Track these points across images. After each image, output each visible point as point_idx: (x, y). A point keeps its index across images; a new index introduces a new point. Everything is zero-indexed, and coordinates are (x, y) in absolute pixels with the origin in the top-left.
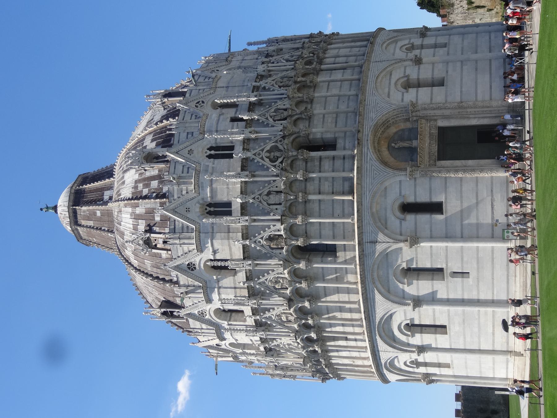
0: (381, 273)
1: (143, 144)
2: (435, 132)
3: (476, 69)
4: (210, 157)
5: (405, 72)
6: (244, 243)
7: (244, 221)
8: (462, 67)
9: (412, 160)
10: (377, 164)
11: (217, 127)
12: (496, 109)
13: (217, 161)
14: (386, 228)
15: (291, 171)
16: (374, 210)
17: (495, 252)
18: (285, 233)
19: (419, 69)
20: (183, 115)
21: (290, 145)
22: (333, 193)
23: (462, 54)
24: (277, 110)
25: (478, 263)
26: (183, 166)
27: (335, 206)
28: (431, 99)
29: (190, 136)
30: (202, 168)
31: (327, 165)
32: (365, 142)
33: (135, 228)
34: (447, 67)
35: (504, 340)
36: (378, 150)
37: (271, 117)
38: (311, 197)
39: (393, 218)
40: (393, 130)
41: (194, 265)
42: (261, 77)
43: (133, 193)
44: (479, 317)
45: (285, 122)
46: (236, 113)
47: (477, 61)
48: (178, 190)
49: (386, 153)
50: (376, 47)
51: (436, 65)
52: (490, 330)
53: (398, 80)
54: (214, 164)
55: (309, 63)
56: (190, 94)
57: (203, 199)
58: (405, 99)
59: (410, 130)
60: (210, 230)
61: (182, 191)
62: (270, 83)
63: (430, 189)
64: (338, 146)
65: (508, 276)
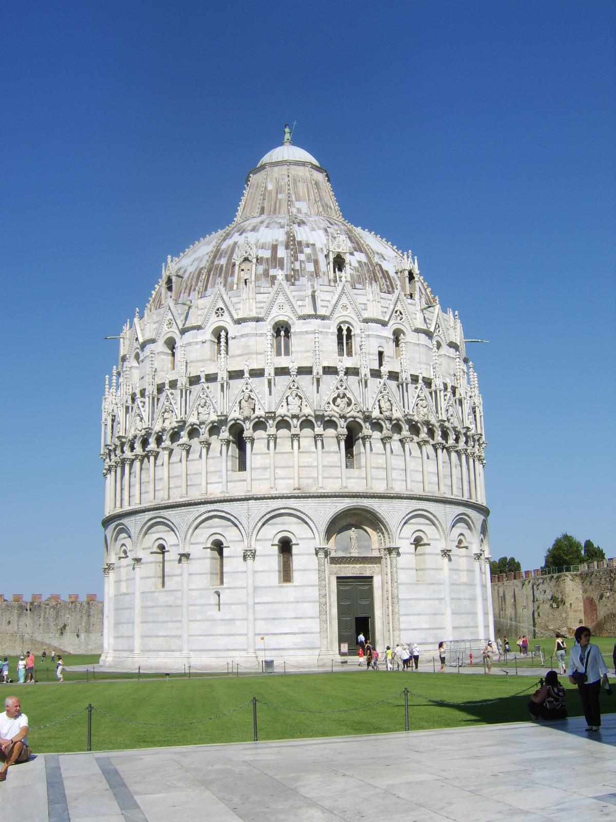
0: (216, 520)
1: (356, 251)
2: (368, 574)
3: (435, 614)
4: (340, 330)
6: (245, 371)
7: (269, 371)
8: (437, 599)
12: (392, 635)
13: (335, 338)
14: (263, 524)
16: (282, 511)
17: (241, 637)
18: (257, 417)
19: (436, 554)
22: (299, 467)
23: (452, 599)
25: (230, 620)
26: (329, 301)
27: (287, 469)
28: (402, 569)
29: (363, 307)
32: (355, 500)
34: (438, 584)
35: (151, 647)
36: (347, 514)
41: (222, 315)
42: (428, 383)
43: (300, 243)
44: (174, 622)
46: (388, 357)
48: (302, 296)
52: (161, 633)
54: (332, 335)
55: (445, 436)
56: (411, 304)
58: (402, 541)
60: (260, 332)
61: (301, 300)
63: (305, 570)
65: (217, 650)
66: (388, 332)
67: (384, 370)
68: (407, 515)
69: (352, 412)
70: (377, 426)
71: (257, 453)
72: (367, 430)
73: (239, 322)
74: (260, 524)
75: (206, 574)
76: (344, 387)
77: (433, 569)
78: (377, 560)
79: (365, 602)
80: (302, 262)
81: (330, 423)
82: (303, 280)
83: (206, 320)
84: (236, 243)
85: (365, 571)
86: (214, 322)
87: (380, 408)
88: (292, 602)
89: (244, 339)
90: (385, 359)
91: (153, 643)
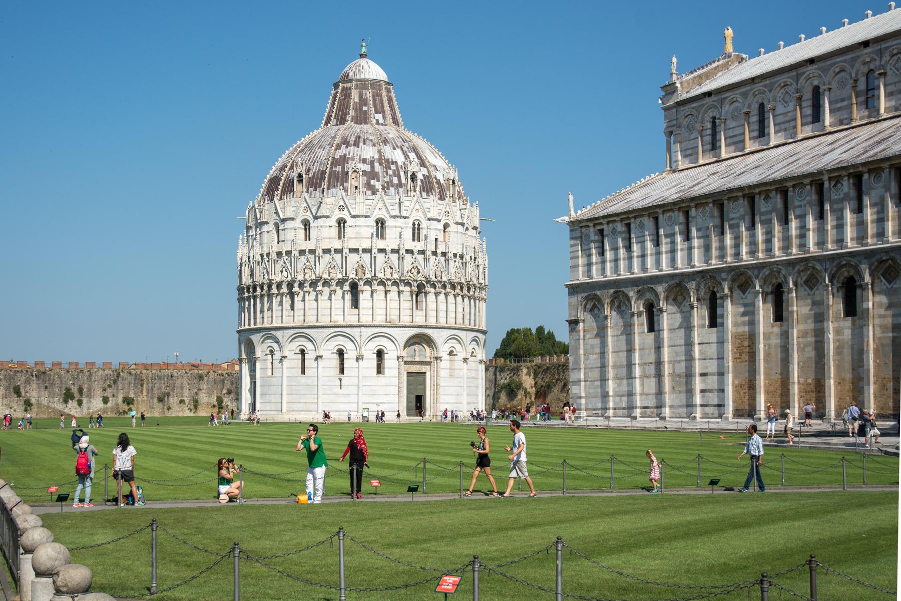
0: (340, 337)
2: (423, 371)
4: (414, 224)
33: (364, 161)
45: (434, 279)
50: (475, 334)
66: (440, 226)
67: (439, 252)
69: (420, 278)
70: (434, 286)
71: (364, 298)
72: (429, 289)
73: (354, 217)
78: (429, 363)
79: (420, 387)
81: (408, 284)
82: (392, 189)
83: (333, 212)
84: (345, 155)
86: (337, 215)
90: (439, 243)
91: (295, 406)
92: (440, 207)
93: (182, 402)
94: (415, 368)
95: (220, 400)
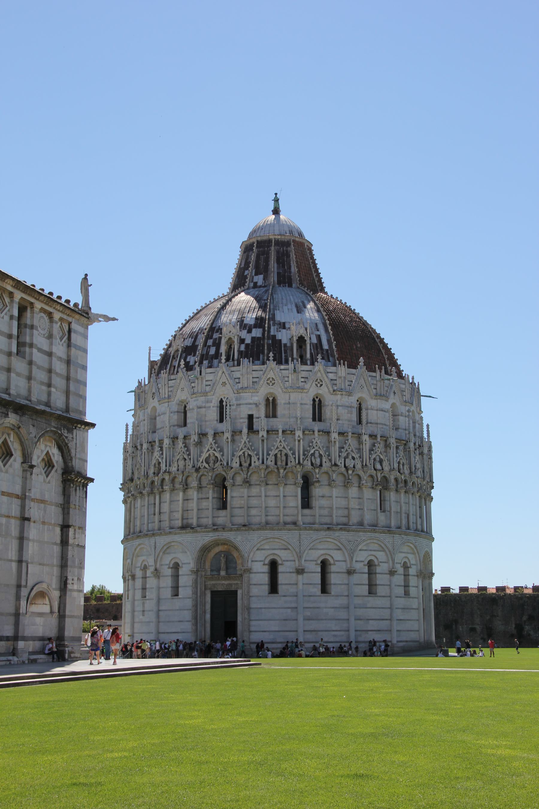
2: (233, 588)
3: (284, 620)
4: (221, 401)
5: (287, 561)
9: (212, 570)
10: (200, 545)
11: (243, 404)
14: (164, 553)
15: (199, 475)
16: (173, 544)
19: (290, 572)
20: (259, 369)
21: (218, 472)
23: (304, 608)
24: (250, 456)
28: (255, 585)
29: (237, 380)
30: (209, 397)
31: (204, 504)
32: (217, 534)
37: (244, 453)
38: (181, 494)
39: (170, 559)
40: (235, 554)
47: (297, 620)
49: (217, 549)
51: (295, 586)
53: (278, 556)
54: (213, 407)
57: (189, 401)
59: (236, 567)
62: (281, 445)
64: (221, 511)
68: (258, 543)
74: (161, 554)
75: (139, 589)
76: (213, 449)
77: (286, 584)
80: (209, 347)
85: (232, 586)
87: (240, 462)
88: (178, 610)
89: (162, 416)
92: (255, 374)
93: (473, 630)
94: (222, 585)
95: (520, 628)
